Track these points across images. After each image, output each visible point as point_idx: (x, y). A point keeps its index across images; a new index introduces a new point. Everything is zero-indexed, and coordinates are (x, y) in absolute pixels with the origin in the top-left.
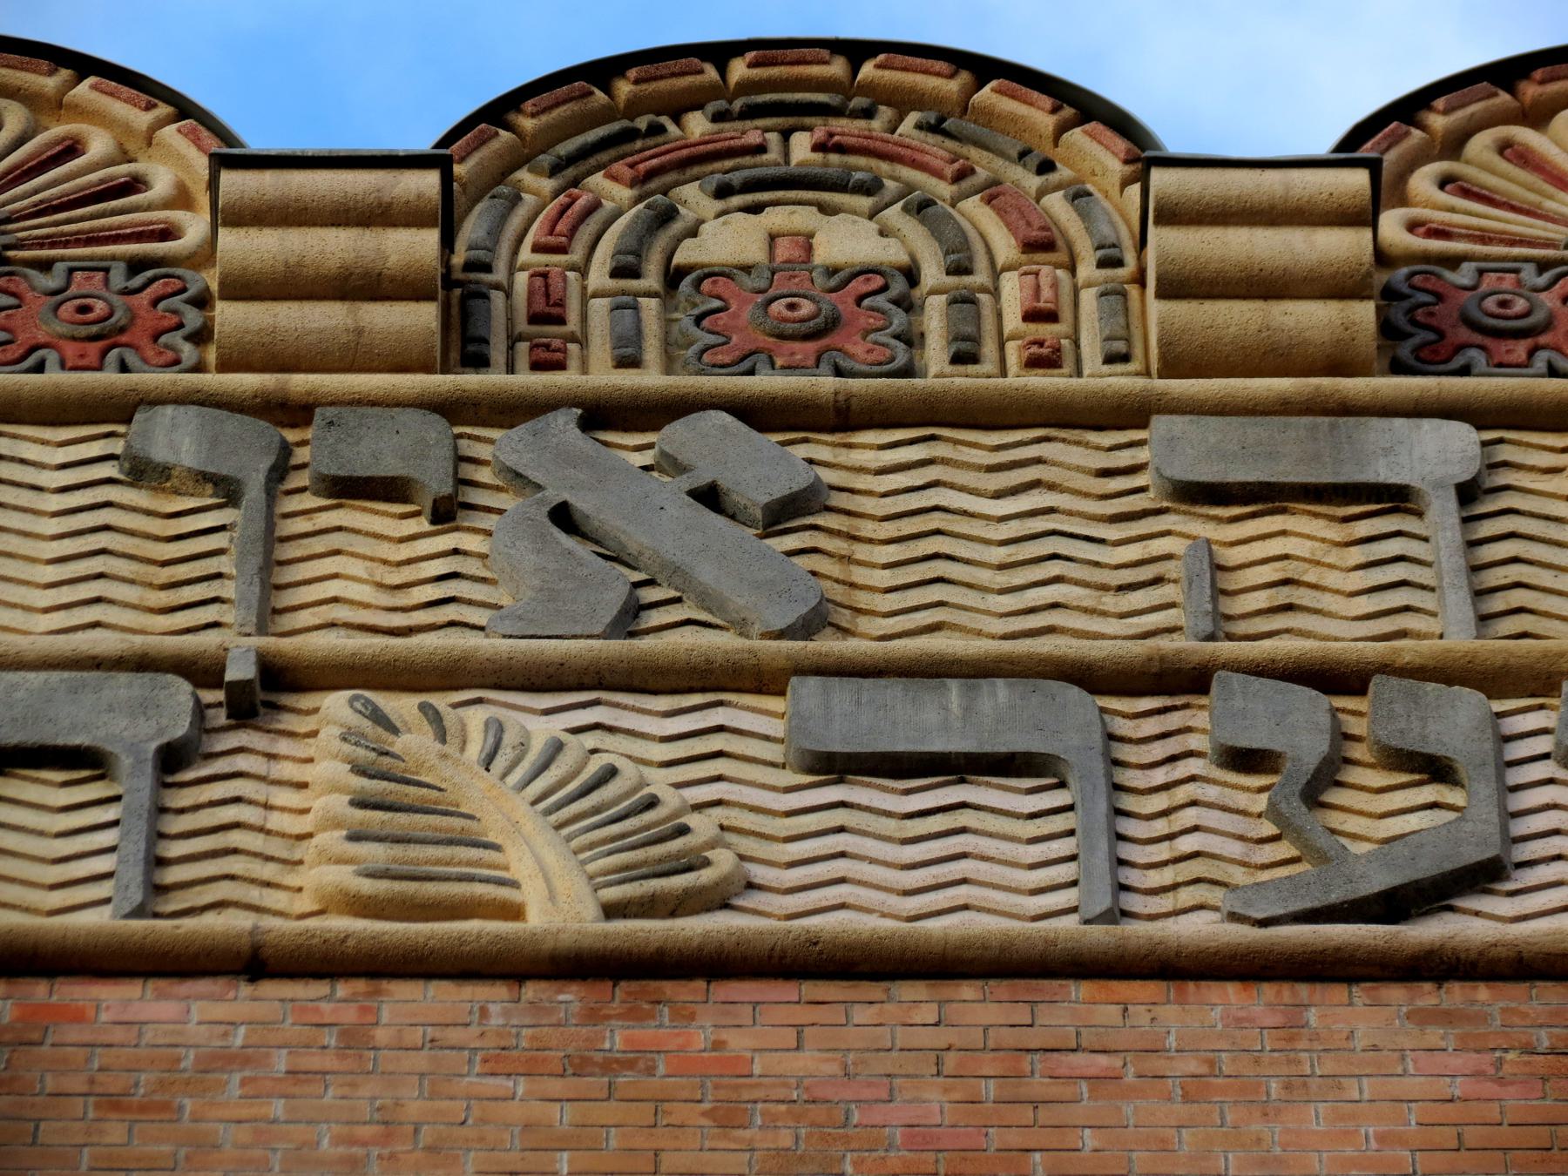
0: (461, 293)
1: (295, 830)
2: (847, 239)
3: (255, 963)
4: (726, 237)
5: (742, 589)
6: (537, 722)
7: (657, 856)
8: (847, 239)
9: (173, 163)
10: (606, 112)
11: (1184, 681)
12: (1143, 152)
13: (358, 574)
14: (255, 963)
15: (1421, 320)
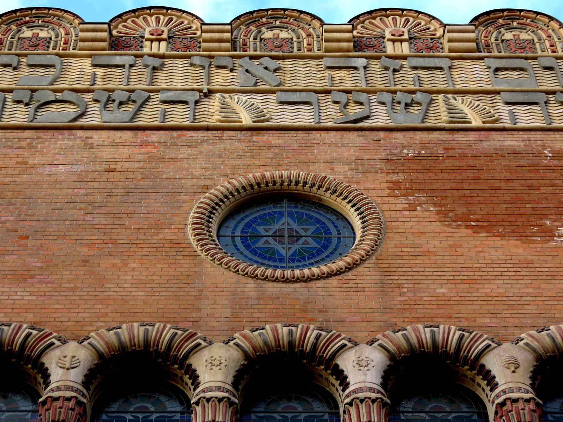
0: (233, 42)
2: (284, 35)
3: (208, 129)
4: (268, 34)
5: (271, 80)
6: (244, 97)
7: (260, 115)
8: (284, 35)
9: (196, 25)
10: (253, 18)
11: (328, 92)
12: (322, 23)
13: (220, 78)
14: (208, 129)
15: (359, 45)
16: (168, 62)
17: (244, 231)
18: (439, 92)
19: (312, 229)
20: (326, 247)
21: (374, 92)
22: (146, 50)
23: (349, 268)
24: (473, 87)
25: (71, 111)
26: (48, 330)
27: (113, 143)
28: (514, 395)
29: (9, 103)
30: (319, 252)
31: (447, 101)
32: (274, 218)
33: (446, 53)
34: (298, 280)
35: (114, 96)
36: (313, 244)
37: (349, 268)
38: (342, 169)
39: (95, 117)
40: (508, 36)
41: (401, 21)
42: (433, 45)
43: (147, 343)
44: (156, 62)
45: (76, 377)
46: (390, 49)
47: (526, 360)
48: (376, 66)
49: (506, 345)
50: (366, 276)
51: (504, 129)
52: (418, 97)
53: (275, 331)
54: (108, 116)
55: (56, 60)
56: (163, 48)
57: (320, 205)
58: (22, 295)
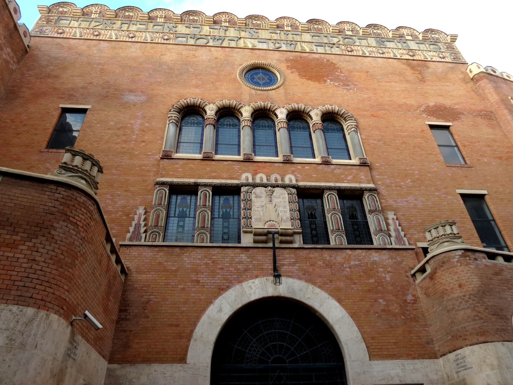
0: (246, 24)
1: (241, 43)
2: (258, 22)
3: (240, 48)
4: (254, 22)
5: (256, 36)
6: (249, 40)
7: (254, 45)
8: (258, 22)
9: (236, 18)
10: (250, 17)
11: (270, 40)
12: (269, 20)
13: (243, 34)
14: (240, 48)
15: (278, 27)
16: (229, 28)
17: (251, 76)
18: (298, 41)
19: (267, 77)
20: (271, 82)
21: (282, 40)
22: (223, 25)
23: (277, 88)
24: (307, 41)
25: (205, 41)
26: (205, 101)
27: (217, 51)
28: (317, 122)
29: (189, 38)
30: (269, 83)
31: (300, 44)
32: (257, 74)
33: (300, 30)
34: (265, 90)
35: (216, 37)
36: (268, 81)
37: (277, 88)
38: (275, 61)
39: (211, 43)
40: (316, 27)
41: (288, 20)
42: (297, 28)
43: (230, 105)
44: (226, 28)
45: (213, 113)
46: (286, 28)
47: (320, 114)
48: (282, 33)
49: (315, 110)
50: (281, 90)
51: (314, 53)
52: (293, 42)
53: (261, 104)
54: (215, 43)
55: (200, 26)
56: (227, 24)
57: (269, 70)
58: (198, 91)
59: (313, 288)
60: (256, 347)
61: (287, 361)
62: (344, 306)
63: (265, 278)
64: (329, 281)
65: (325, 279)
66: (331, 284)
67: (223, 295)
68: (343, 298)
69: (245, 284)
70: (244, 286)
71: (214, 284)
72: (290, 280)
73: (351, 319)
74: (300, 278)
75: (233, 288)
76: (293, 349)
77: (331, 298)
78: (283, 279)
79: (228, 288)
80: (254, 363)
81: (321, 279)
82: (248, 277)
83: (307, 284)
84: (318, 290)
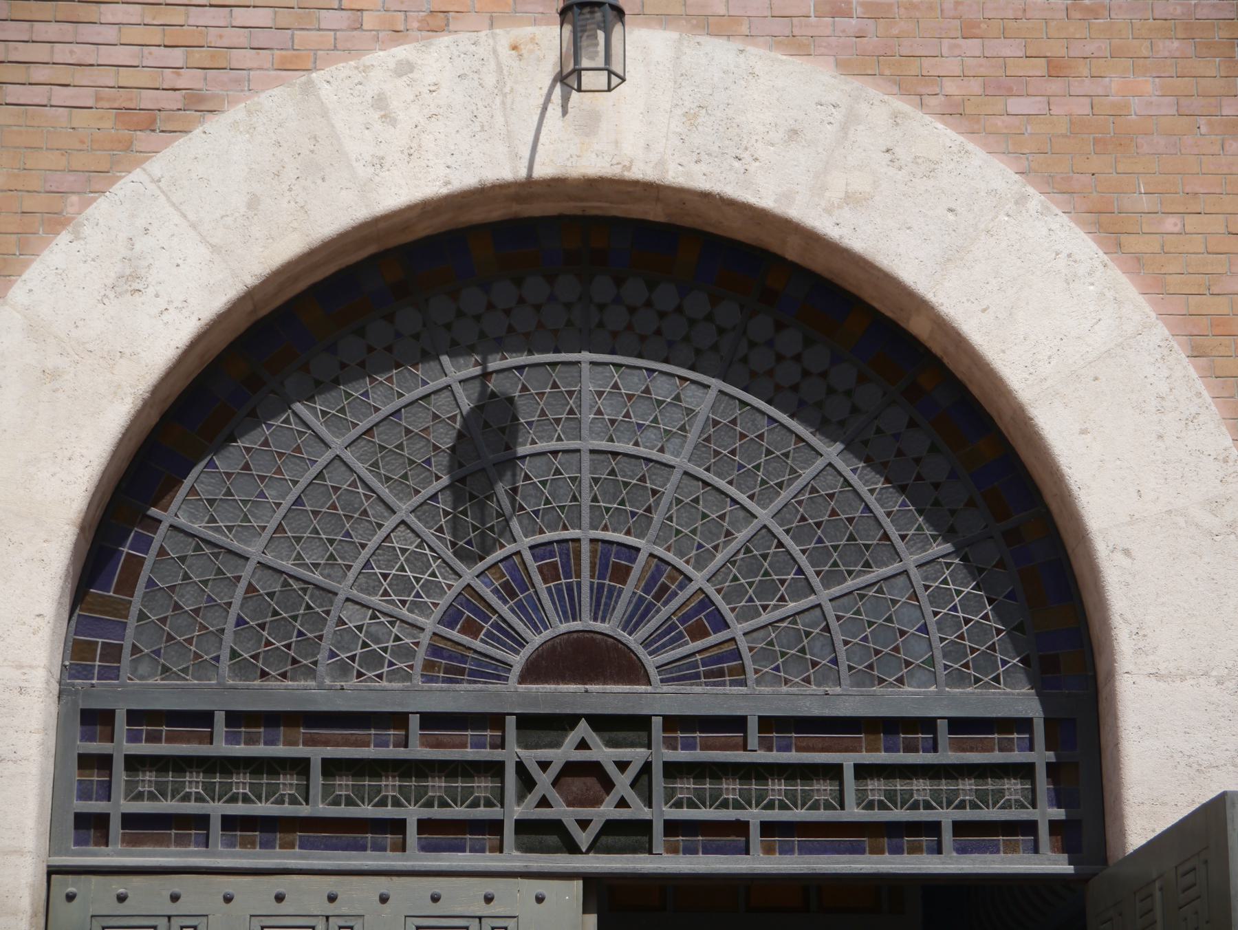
59: (896, 118)
60: (417, 561)
61: (651, 662)
62: (1136, 265)
63: (504, 36)
64: (1040, 67)
65: (1010, 49)
66: (1055, 86)
67: (156, 166)
68: (1145, 203)
69: (334, 83)
70: (326, 91)
71: (81, 76)
72: (717, 56)
73: (1186, 369)
74: (796, 43)
75: (236, 113)
76: (699, 578)
77: (1036, 200)
78: (644, 45)
79: (199, 106)
80: (394, 675)
81: (973, 46)
82: (369, 20)
83: (856, 83)
84: (934, 135)
